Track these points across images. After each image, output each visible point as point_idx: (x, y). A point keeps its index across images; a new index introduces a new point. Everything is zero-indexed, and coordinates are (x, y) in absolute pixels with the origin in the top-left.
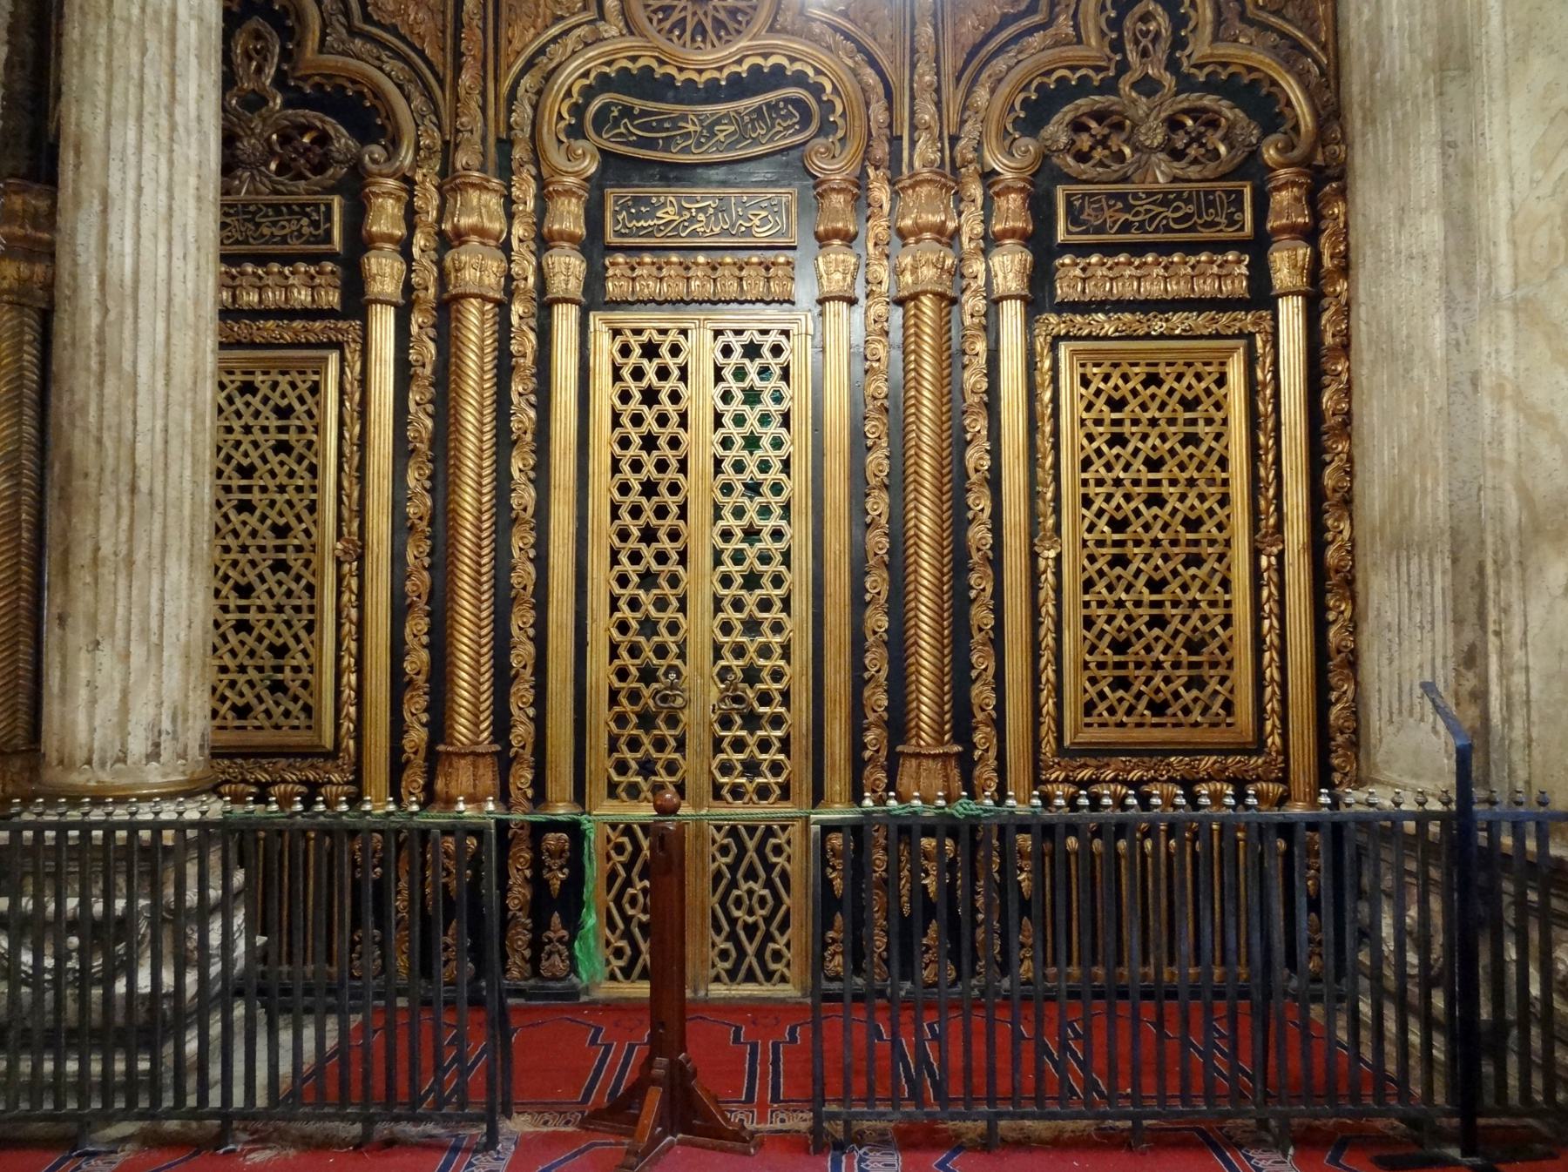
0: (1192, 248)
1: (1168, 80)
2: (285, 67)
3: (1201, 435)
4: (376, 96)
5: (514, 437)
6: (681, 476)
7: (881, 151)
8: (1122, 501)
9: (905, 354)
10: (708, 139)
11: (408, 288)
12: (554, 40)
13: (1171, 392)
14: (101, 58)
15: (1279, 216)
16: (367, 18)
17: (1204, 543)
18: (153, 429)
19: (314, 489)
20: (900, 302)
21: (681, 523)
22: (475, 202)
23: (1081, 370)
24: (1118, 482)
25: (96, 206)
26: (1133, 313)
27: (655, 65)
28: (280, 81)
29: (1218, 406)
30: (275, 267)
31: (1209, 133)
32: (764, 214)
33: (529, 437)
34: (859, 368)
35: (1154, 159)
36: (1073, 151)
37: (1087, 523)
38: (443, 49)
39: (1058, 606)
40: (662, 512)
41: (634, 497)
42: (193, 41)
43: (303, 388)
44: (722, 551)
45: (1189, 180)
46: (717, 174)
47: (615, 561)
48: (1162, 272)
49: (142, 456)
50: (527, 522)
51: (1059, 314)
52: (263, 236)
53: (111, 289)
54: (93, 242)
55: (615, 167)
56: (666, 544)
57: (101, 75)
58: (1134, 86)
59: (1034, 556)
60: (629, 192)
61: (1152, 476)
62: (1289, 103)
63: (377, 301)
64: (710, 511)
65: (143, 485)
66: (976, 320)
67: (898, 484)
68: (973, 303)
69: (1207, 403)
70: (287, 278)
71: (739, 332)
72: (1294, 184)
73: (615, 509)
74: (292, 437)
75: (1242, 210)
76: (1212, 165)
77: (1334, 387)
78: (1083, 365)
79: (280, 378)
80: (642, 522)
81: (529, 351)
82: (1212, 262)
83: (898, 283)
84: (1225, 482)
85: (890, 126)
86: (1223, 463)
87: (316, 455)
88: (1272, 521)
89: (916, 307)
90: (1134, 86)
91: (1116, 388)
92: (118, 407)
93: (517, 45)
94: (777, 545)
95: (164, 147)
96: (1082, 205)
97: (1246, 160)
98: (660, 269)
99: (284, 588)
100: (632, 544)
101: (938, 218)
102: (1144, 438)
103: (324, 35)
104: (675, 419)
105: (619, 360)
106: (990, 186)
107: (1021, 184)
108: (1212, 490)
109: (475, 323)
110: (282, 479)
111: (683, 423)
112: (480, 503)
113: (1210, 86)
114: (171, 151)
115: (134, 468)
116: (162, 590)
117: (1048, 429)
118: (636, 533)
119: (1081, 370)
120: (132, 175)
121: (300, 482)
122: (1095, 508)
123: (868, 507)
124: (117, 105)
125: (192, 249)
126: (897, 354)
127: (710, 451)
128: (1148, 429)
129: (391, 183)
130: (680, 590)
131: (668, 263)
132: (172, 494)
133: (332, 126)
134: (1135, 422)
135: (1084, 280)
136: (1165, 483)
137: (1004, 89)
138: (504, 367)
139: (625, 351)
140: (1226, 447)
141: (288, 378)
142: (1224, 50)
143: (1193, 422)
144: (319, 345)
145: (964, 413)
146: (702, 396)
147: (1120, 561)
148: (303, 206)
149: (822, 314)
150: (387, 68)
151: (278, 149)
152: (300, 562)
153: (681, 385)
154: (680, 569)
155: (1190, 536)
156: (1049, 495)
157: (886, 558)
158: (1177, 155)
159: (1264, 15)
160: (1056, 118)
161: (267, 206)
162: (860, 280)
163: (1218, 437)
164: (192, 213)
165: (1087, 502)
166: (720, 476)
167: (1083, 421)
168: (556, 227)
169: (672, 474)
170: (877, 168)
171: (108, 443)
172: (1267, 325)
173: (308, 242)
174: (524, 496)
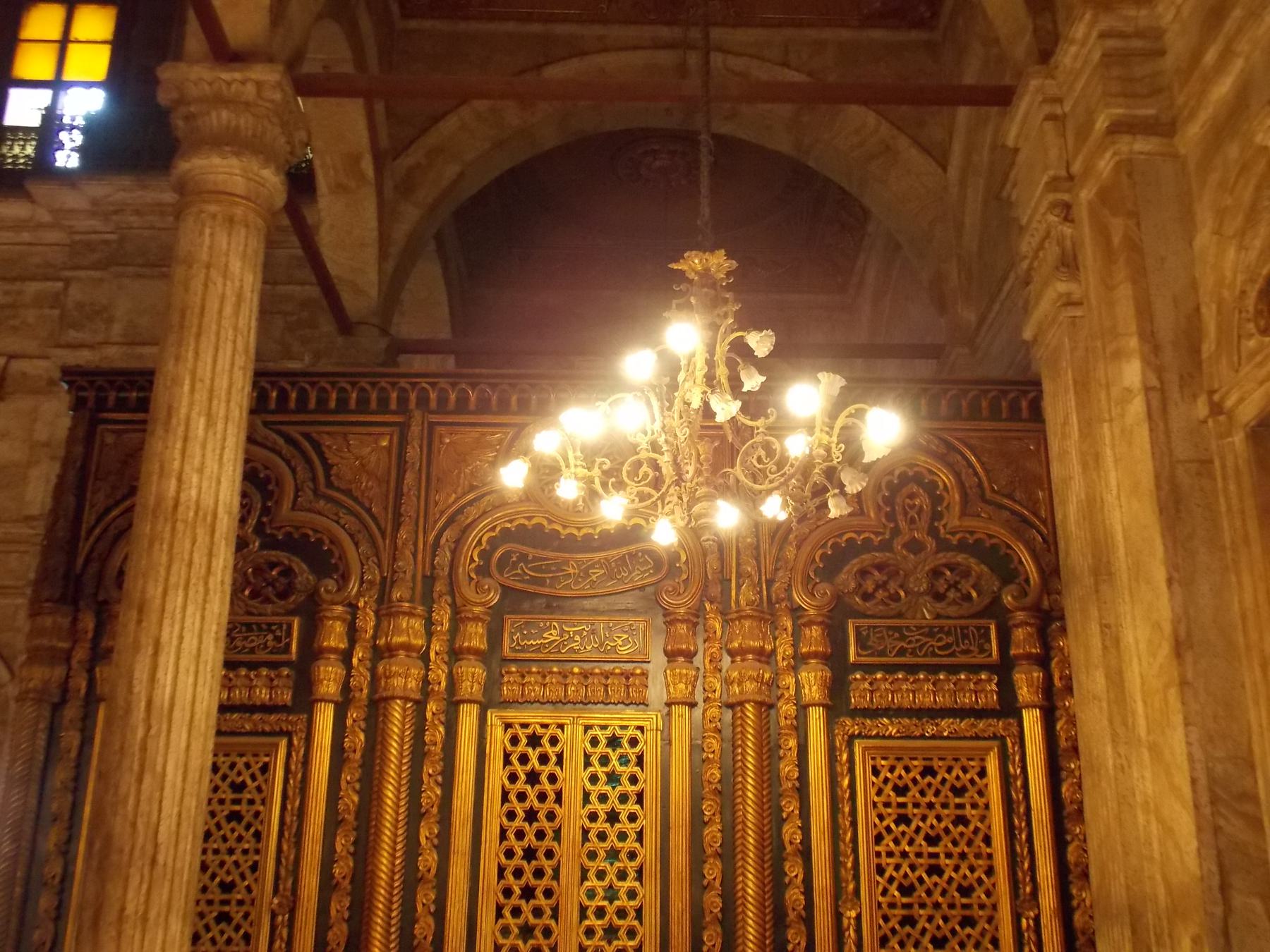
0: (953, 669)
1: (930, 544)
2: (265, 519)
3: (969, 817)
4: (332, 542)
5: (423, 810)
6: (556, 844)
7: (715, 591)
8: (908, 870)
9: (734, 747)
10: (584, 579)
11: (346, 688)
12: (471, 503)
13: (944, 781)
14: (165, 547)
15: (1018, 647)
16: (329, 484)
17: (976, 907)
18: (170, 816)
19: (257, 852)
20: (731, 706)
21: (555, 883)
22: (404, 625)
23: (871, 762)
24: (904, 855)
25: (150, 650)
26: (910, 718)
27: (545, 523)
28: (259, 529)
29: (981, 793)
30: (243, 672)
31: (963, 582)
32: (625, 636)
33: (435, 810)
34: (697, 758)
35: (921, 600)
36: (861, 591)
37: (880, 888)
38: (386, 509)
40: (539, 873)
41: (517, 861)
42: (225, 530)
43: (256, 768)
44: (587, 908)
45: (949, 617)
46: (587, 604)
47: (499, 914)
48: (931, 687)
49: (163, 836)
50: (430, 881)
51: (853, 718)
52: (236, 647)
53: (155, 713)
54: (145, 677)
55: (513, 599)
56: (541, 901)
57: (164, 559)
58: (905, 546)
59: (838, 916)
60: (522, 618)
61: (931, 850)
62: (1021, 562)
63: (321, 700)
64: (578, 874)
65: (161, 859)
66: (789, 722)
67: (729, 853)
68: (787, 708)
69: (972, 792)
70: (251, 680)
71: (604, 727)
72: (1027, 624)
73: (501, 871)
74: (242, 808)
75: (989, 641)
76: (966, 605)
77: (1070, 781)
78: (873, 759)
79: (238, 759)
80: (523, 881)
81: (439, 740)
82: (968, 680)
83: (728, 690)
84: (990, 856)
85: (722, 571)
86: (987, 840)
87: (262, 822)
88: (1028, 889)
89: (742, 712)
90: (905, 546)
91: (900, 777)
92: (150, 800)
93: (441, 507)
94: (632, 903)
95: (200, 606)
96: (868, 635)
97: (992, 603)
98: (544, 677)
99: (225, 936)
100: (515, 900)
101: (757, 644)
102: (924, 818)
103: (296, 497)
104: (552, 796)
105: (509, 748)
106: (799, 618)
107: (820, 619)
108: (980, 862)
109: (397, 717)
110: (232, 843)
111: (559, 798)
112: (393, 865)
113: (962, 547)
114: (204, 609)
115: (156, 846)
116: (164, 942)
117: (847, 810)
118: (517, 891)
119: (871, 762)
120: (177, 627)
121: (246, 846)
122: (887, 875)
123: (705, 872)
124: (173, 580)
125: (209, 676)
126: (727, 746)
127: (579, 823)
128: (927, 812)
129: (339, 609)
130: (552, 940)
131: (551, 673)
132: (179, 865)
133: (299, 566)
134: (916, 805)
135: (872, 692)
136: (942, 856)
137: (806, 549)
138: (418, 753)
139: (515, 740)
140: (989, 827)
141: (244, 759)
142: (970, 523)
144: (272, 734)
145: (781, 795)
146: (574, 777)
147: (909, 921)
148: (270, 625)
149: (669, 714)
150: (342, 522)
151: (252, 580)
152: (241, 914)
153: (558, 769)
154: (553, 923)
155: (964, 901)
156: (849, 865)
157: (720, 915)
158: (939, 597)
159: (999, 499)
160: (846, 569)
161: (242, 624)
162: (699, 688)
164: (212, 650)
165: (880, 870)
166: (587, 845)
167: (875, 804)
168: (466, 644)
169: (548, 842)
170: (711, 603)
171: (140, 827)
172: (1015, 730)
173: (271, 652)
174: (429, 859)
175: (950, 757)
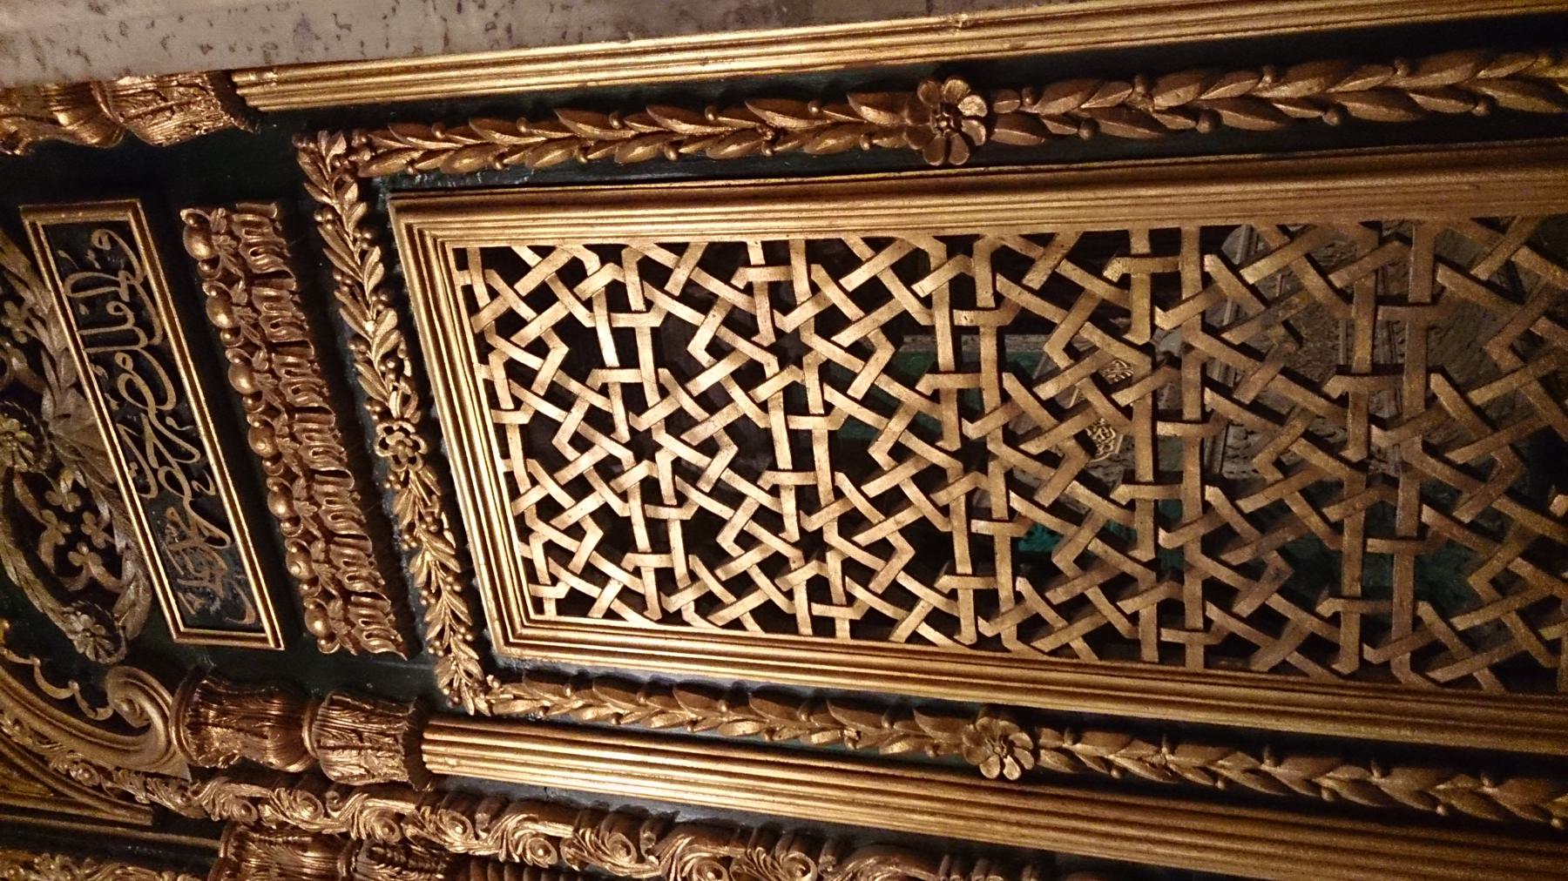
39: (1175, 735)
84: (776, 253)
86: (723, 259)
143: (625, 340)
163: (654, 274)
175: (481, 373)
